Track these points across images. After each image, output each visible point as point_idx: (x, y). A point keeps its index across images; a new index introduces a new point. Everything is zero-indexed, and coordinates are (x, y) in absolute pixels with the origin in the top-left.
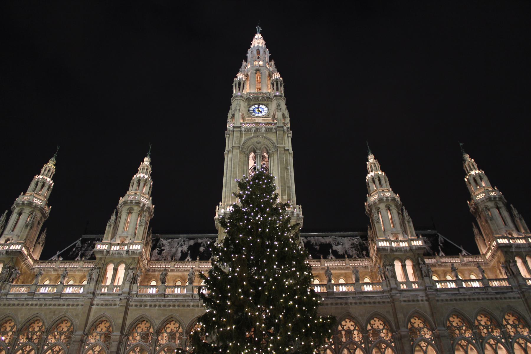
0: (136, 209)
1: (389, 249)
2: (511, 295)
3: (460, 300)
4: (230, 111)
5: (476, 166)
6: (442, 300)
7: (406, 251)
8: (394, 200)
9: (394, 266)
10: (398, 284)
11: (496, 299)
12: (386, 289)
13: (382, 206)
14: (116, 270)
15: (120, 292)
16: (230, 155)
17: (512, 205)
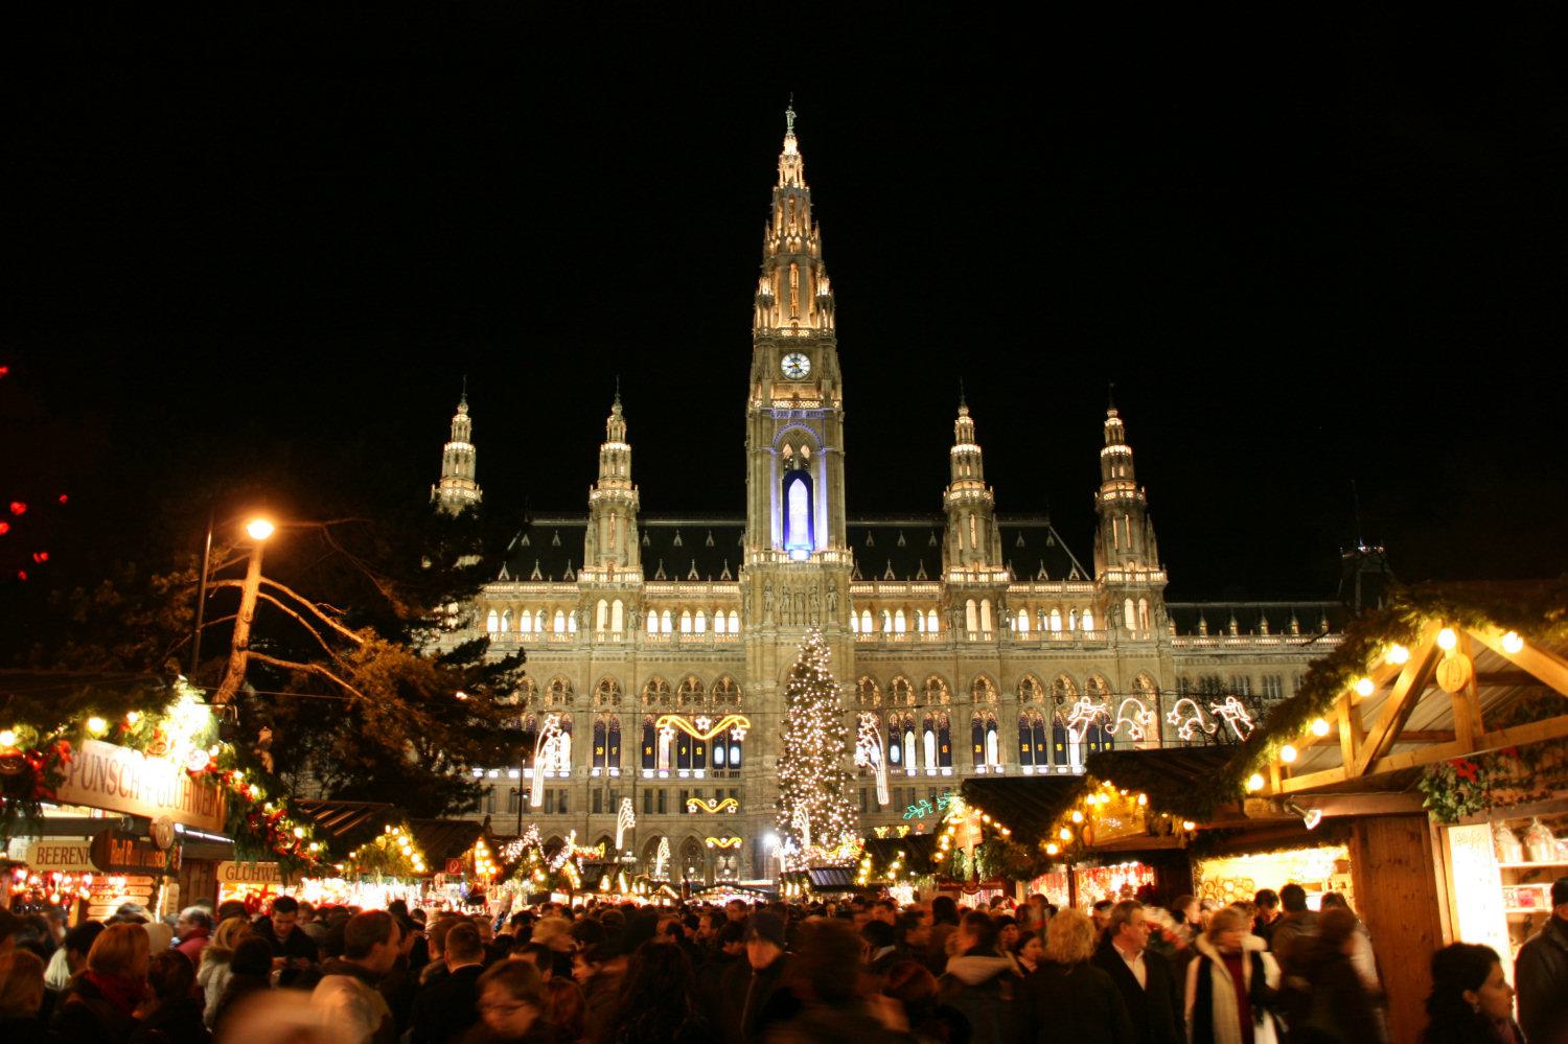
0: (621, 511)
1: (962, 585)
2: (1103, 653)
3: (1040, 657)
4: (753, 365)
5: (1121, 437)
6: (1017, 658)
7: (984, 587)
8: (983, 502)
9: (964, 608)
10: (966, 634)
11: (1084, 657)
12: (951, 640)
13: (964, 512)
14: (610, 609)
15: (623, 642)
16: (758, 462)
17: (1148, 515)
